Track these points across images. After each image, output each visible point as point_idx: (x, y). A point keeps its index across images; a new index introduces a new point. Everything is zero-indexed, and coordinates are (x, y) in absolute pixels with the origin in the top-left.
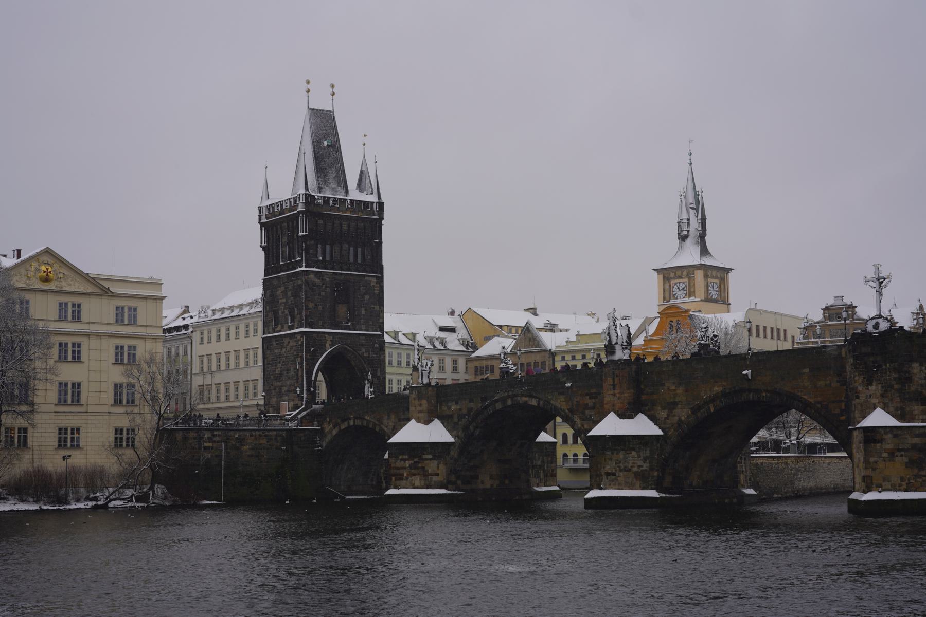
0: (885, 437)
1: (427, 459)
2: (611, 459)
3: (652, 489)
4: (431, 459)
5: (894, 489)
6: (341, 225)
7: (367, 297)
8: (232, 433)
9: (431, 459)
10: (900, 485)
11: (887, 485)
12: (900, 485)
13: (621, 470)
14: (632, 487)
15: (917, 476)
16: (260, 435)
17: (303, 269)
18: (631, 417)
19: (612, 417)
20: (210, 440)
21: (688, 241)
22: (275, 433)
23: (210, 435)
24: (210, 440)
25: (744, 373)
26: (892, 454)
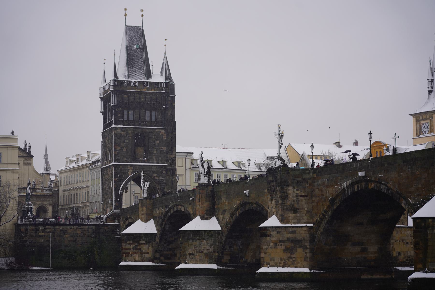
0: (272, 233)
1: (142, 244)
2: (192, 245)
3: (214, 264)
4: (144, 244)
5: (276, 265)
6: (140, 98)
7: (158, 142)
8: (57, 227)
9: (144, 244)
10: (280, 263)
11: (272, 263)
12: (280, 263)
13: (197, 252)
14: (203, 263)
15: (290, 258)
16: (76, 228)
17: (113, 126)
18: (207, 219)
19: (198, 218)
20: (43, 231)
21: (432, 94)
22: (87, 227)
23: (43, 228)
24: (43, 231)
25: (244, 192)
26: (276, 244)
